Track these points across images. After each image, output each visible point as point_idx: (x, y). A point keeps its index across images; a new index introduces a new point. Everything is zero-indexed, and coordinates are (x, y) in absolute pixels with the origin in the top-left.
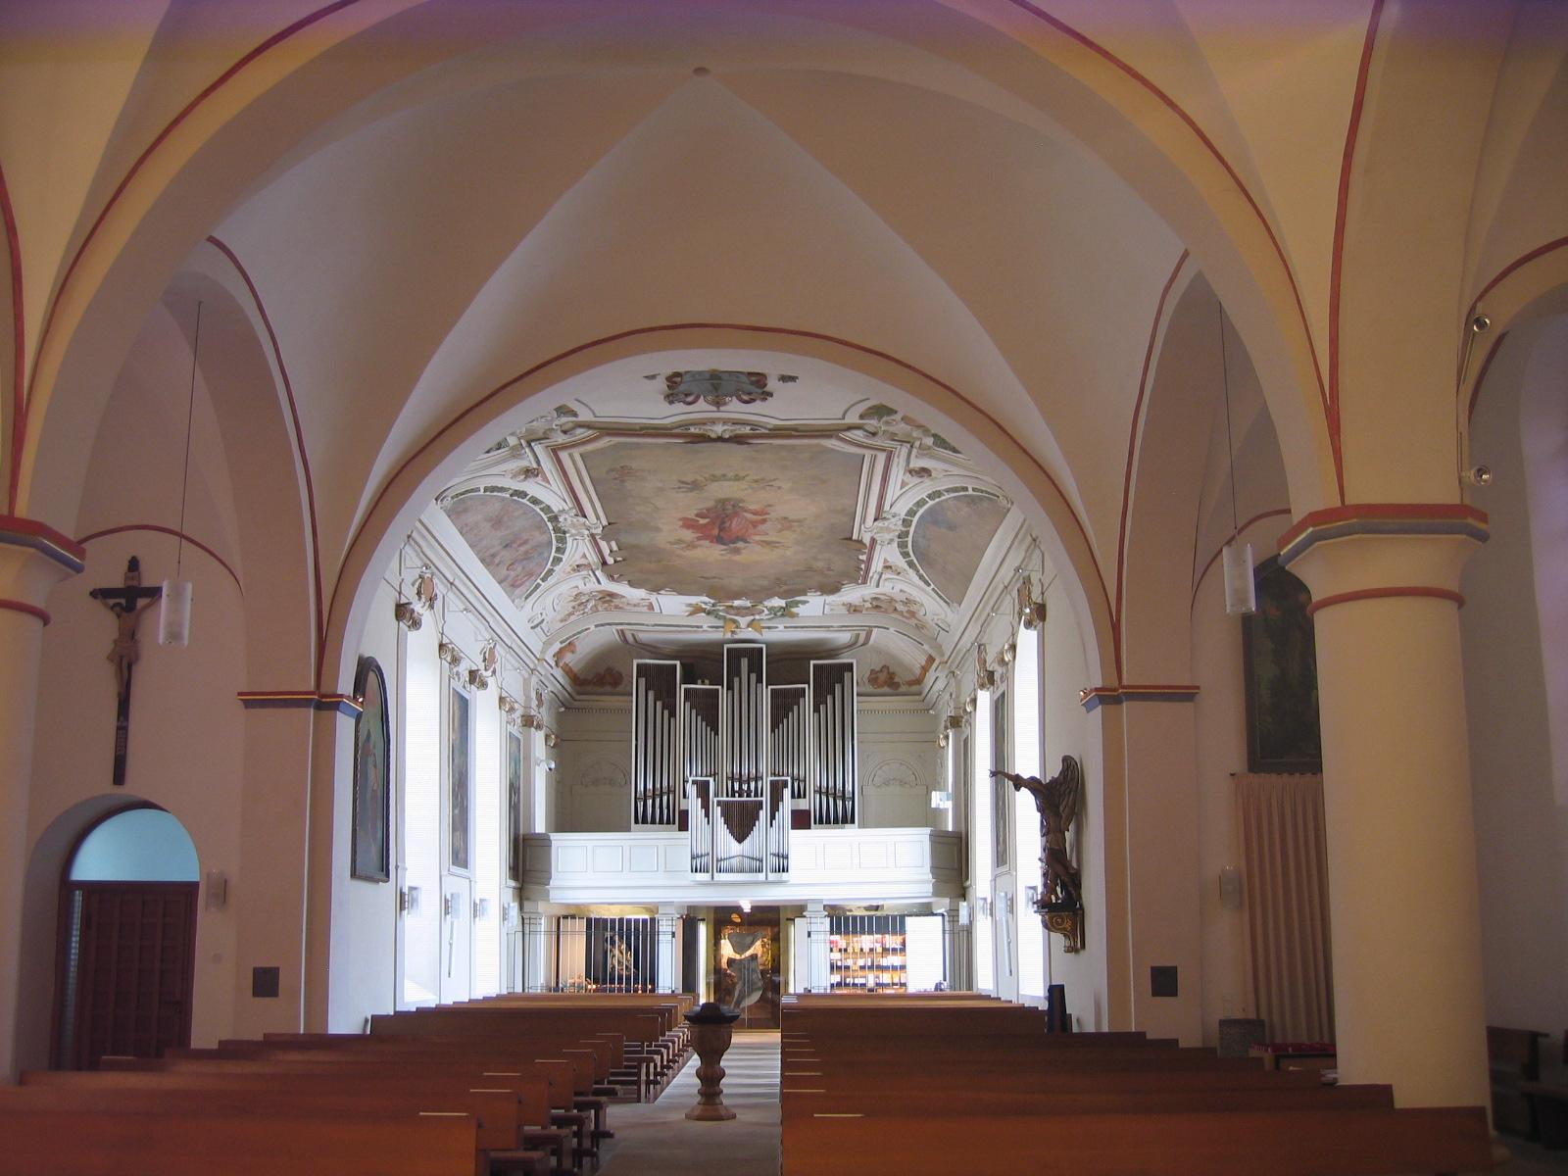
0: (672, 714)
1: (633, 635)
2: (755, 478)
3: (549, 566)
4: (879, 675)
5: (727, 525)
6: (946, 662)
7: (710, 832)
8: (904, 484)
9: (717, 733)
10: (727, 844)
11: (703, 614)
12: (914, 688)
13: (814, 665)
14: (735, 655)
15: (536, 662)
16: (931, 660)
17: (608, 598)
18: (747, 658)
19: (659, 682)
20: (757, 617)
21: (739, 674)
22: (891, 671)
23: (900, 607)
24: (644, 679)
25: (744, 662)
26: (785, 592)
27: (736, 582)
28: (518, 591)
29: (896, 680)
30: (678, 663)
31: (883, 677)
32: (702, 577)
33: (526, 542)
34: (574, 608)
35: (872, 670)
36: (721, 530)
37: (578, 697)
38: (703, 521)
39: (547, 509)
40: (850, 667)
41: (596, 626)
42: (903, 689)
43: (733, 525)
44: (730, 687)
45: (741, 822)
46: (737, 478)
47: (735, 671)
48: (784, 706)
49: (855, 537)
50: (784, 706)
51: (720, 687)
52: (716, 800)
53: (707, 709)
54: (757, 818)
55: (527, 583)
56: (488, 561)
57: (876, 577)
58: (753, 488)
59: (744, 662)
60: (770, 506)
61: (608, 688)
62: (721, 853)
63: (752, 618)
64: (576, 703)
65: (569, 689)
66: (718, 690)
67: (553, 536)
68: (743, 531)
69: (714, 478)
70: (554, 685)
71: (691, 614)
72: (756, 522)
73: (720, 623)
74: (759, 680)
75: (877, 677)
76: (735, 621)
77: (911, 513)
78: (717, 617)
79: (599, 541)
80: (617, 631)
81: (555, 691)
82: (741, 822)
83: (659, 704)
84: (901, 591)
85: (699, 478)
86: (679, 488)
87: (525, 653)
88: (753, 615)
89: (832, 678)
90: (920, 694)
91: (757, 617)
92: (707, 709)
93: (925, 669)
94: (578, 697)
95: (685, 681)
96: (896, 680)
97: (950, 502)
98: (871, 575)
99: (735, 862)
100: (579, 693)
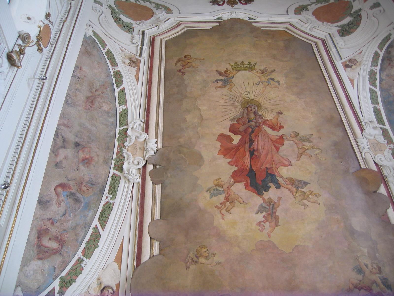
2: (262, 68)
3: (79, 254)
5: (255, 146)
8: (352, 81)
28: (36, 264)
33: (87, 161)
36: (252, 153)
38: (236, 139)
39: (124, 114)
43: (260, 148)
46: (251, 68)
49: (363, 167)
56: (60, 142)
58: (263, 83)
60: (280, 113)
67: (112, 171)
68: (269, 156)
69: (239, 67)
72: (276, 141)
77: (377, 112)
79: (148, 178)
85: (230, 68)
86: (217, 81)
97: (384, 78)
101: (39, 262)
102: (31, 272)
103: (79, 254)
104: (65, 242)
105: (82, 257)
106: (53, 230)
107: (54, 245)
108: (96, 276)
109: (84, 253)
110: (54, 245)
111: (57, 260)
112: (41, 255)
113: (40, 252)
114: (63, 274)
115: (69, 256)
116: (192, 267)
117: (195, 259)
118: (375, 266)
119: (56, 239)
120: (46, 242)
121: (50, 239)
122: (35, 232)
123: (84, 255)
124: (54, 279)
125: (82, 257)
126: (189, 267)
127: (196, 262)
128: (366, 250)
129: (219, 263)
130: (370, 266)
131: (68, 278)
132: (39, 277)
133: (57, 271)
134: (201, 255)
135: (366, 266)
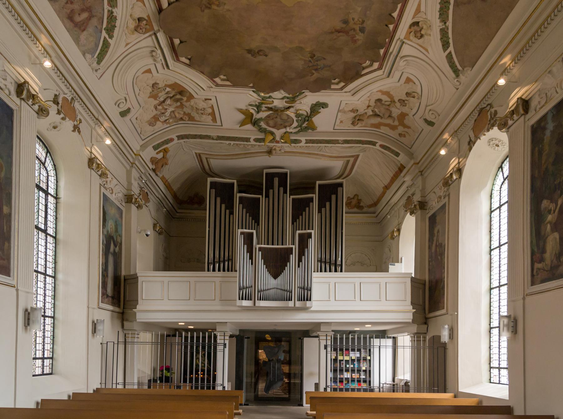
0: (231, 213)
1: (207, 158)
3: (106, 7)
4: (352, 200)
6: (418, 163)
7: (250, 270)
9: (258, 224)
10: (266, 280)
11: (249, 127)
12: (372, 209)
13: (320, 186)
14: (270, 177)
15: (134, 155)
16: (401, 168)
17: (178, 96)
18: (277, 179)
19: (224, 193)
20: (288, 129)
21: (272, 188)
22: (359, 198)
23: (396, 112)
24: (214, 190)
25: (276, 180)
26: (317, 81)
27: (273, 62)
28: (84, 36)
29: (362, 204)
30: (235, 181)
31: (354, 202)
32: (249, 51)
34: (156, 108)
35: (349, 197)
37: (179, 211)
40: (341, 185)
41: (180, 137)
42: (365, 209)
44: (267, 196)
45: (277, 263)
47: (270, 186)
48: (300, 208)
50: (300, 208)
51: (260, 196)
52: (258, 246)
53: (252, 208)
54: (289, 260)
55: (90, 29)
57: (395, 53)
59: (276, 180)
61: (196, 206)
62: (260, 285)
63: (283, 130)
64: (178, 214)
65: (171, 201)
66: (259, 198)
70: (167, 205)
71: (243, 123)
73: (261, 136)
74: (285, 192)
75: (351, 202)
76: (272, 133)
78: (261, 130)
80: (196, 153)
81: (160, 197)
82: (277, 263)
83: (223, 206)
84: (408, 80)
87: (118, 138)
88: (285, 127)
89: (330, 191)
90: (374, 213)
91: (288, 129)
92: (252, 208)
93: (387, 188)
94: (179, 211)
95: (240, 192)
96: (362, 204)
98: (391, 50)
99: (272, 292)
100: (179, 209)
101: (85, 33)
102: (85, 41)
103: (106, 7)
104: (90, 7)
105: (110, 9)
106: (76, 7)
107: (85, 15)
108: (128, 15)
109: (109, 4)
110: (85, 15)
111: (94, 21)
112: (82, 28)
113: (80, 28)
114: (104, 26)
115: (100, 13)
116: (207, 11)
117: (209, 6)
118: (360, 20)
119: (83, 10)
120: (78, 19)
121: (79, 14)
122: (67, 21)
123: (111, 7)
124: (101, 32)
125: (110, 9)
126: (204, 11)
127: (210, 8)
128: (359, 9)
129: (229, 10)
130: (356, 20)
131: (109, 26)
132: (91, 39)
133: (99, 27)
134: (213, 3)
135: (353, 19)
